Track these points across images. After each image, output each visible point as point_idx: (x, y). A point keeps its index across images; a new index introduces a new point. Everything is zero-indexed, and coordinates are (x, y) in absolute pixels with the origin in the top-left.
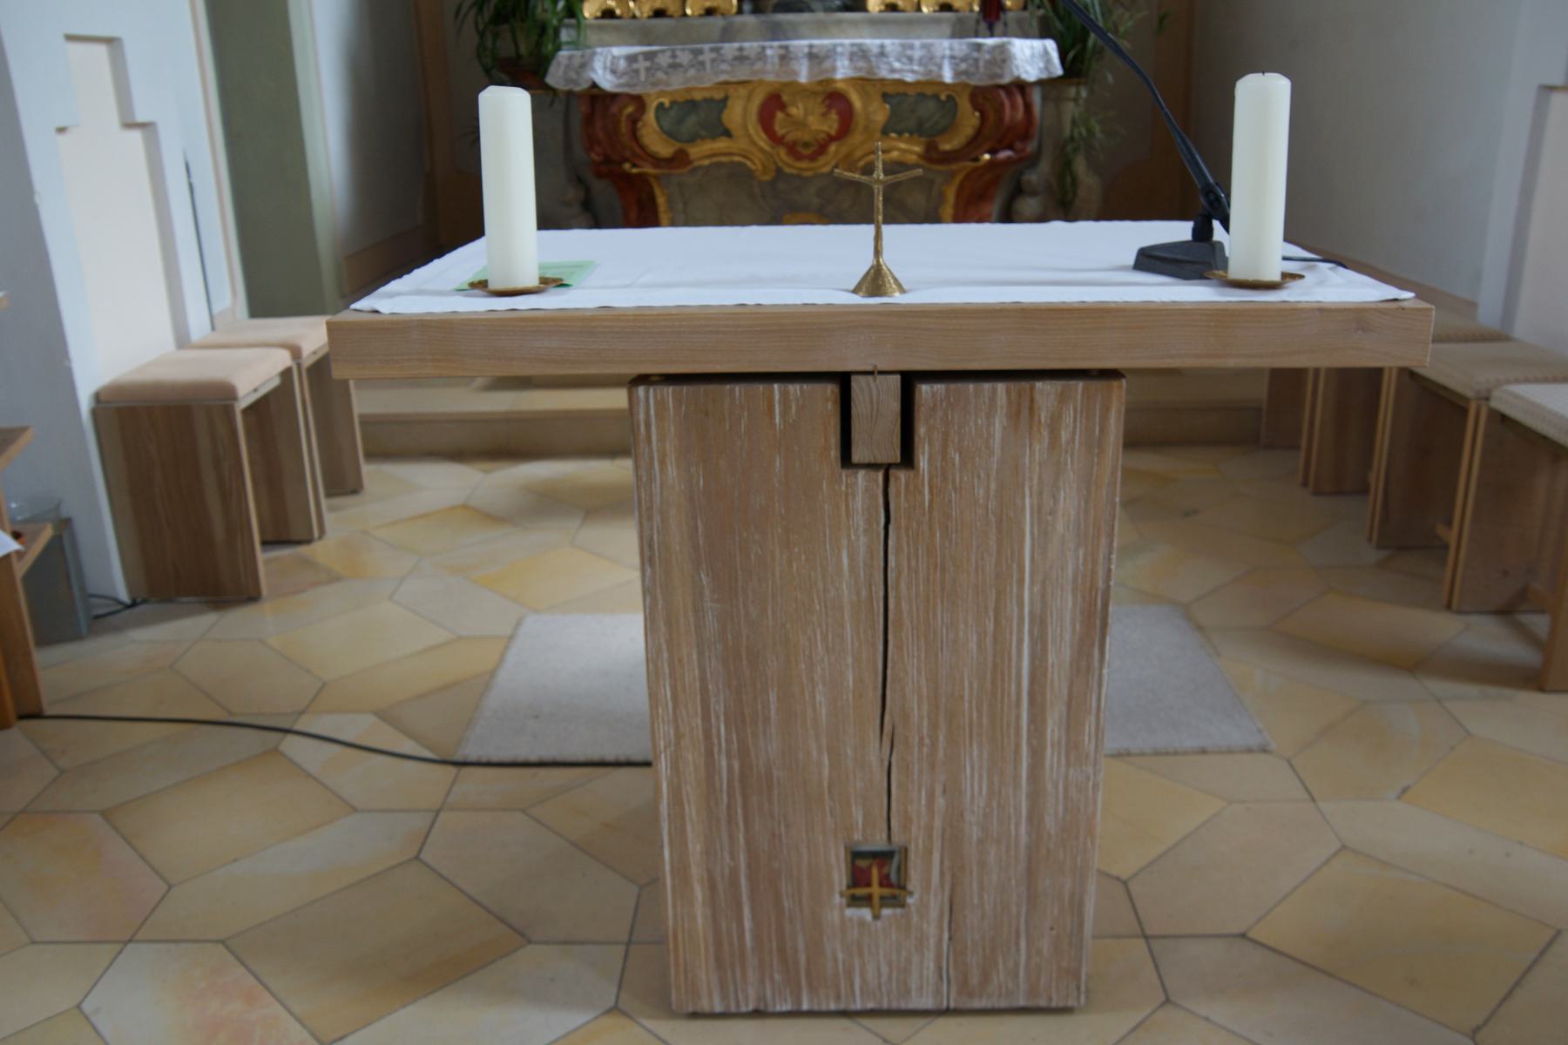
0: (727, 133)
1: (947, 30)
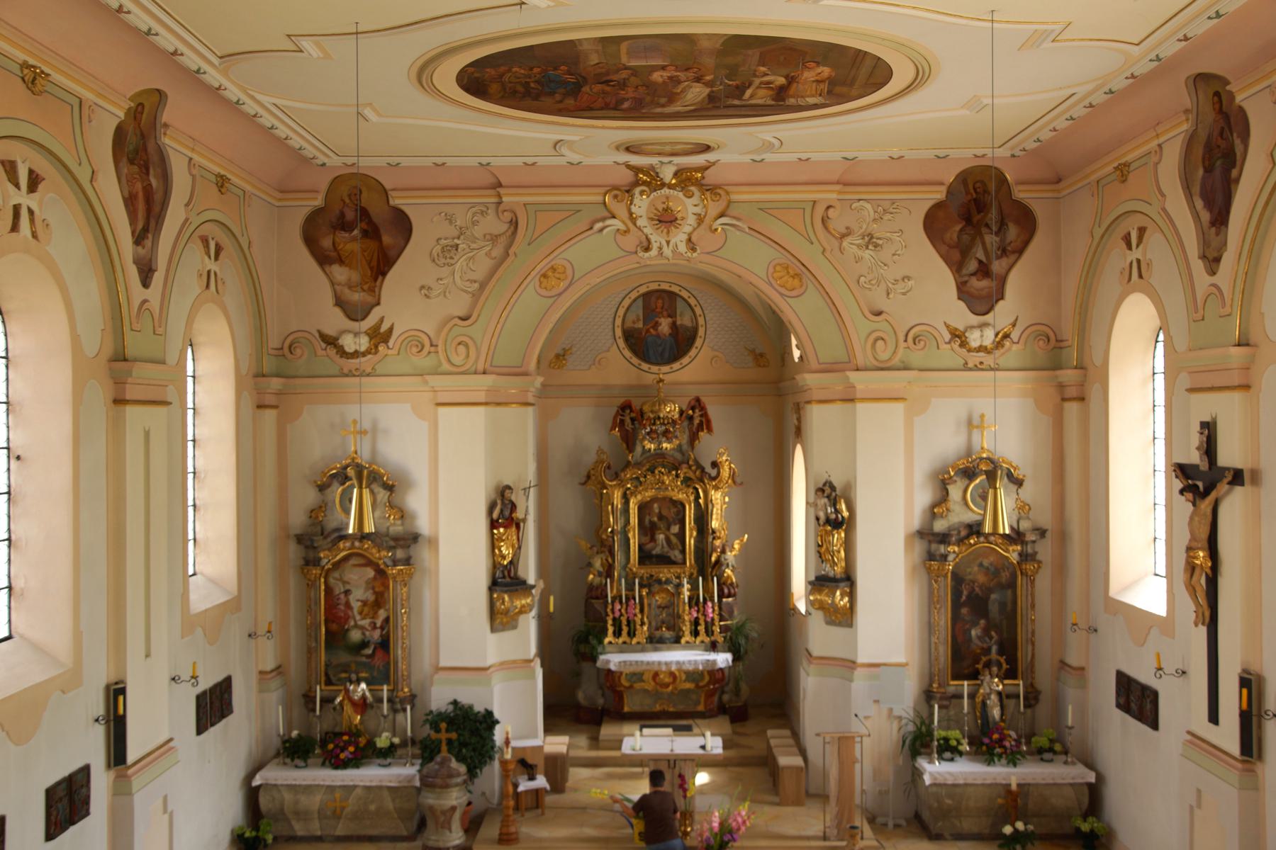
0: (643, 681)
1: (703, 648)
